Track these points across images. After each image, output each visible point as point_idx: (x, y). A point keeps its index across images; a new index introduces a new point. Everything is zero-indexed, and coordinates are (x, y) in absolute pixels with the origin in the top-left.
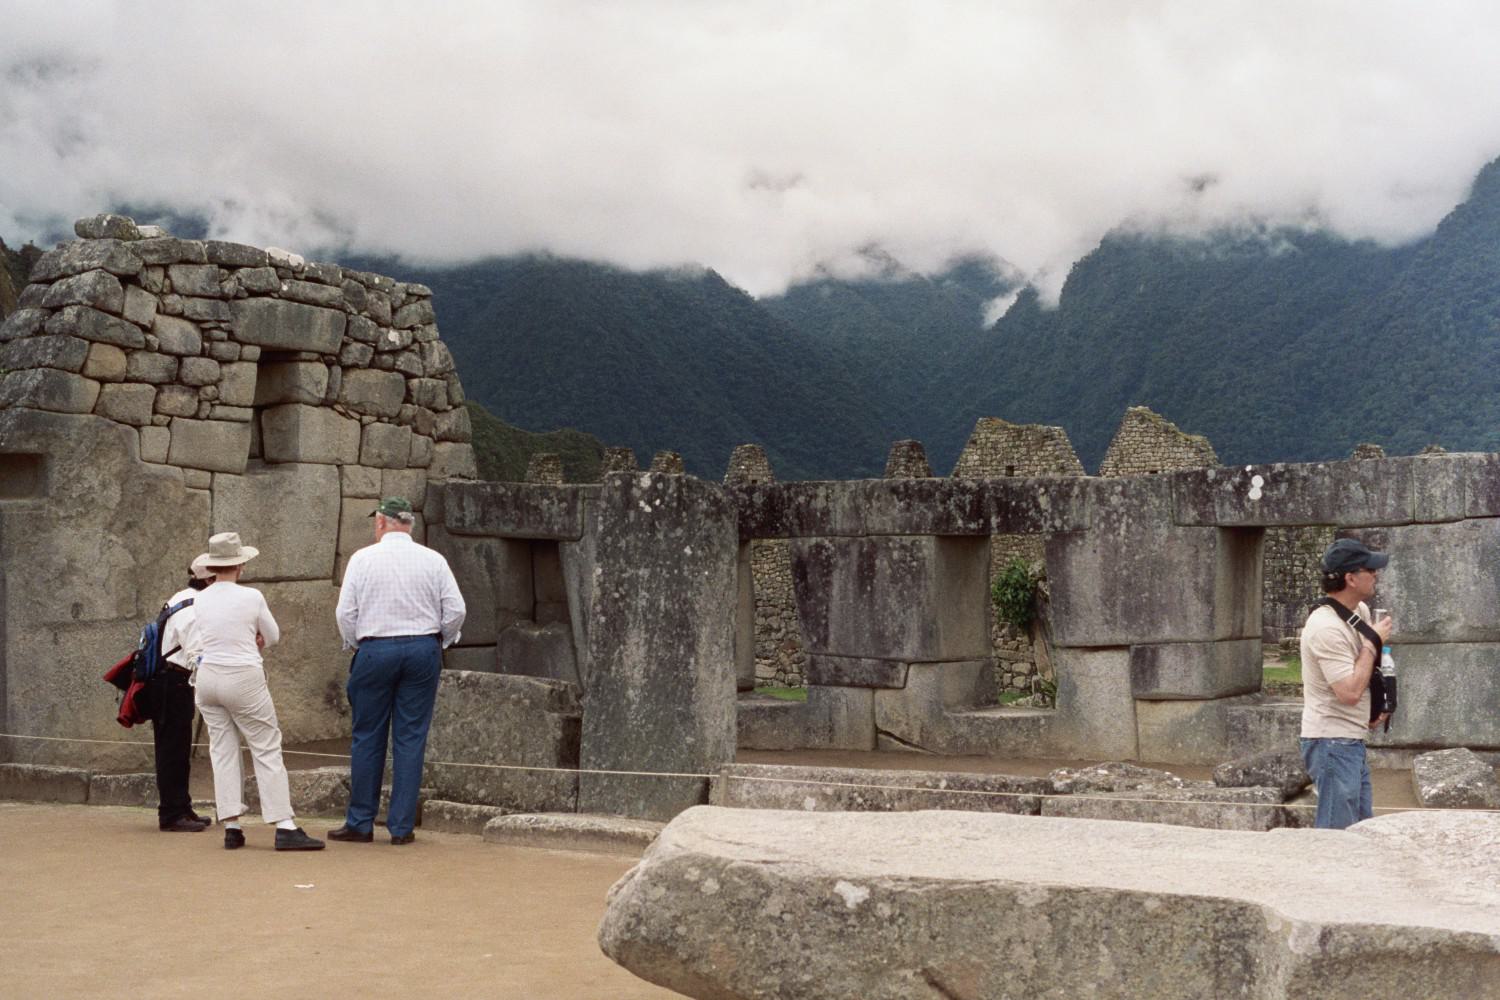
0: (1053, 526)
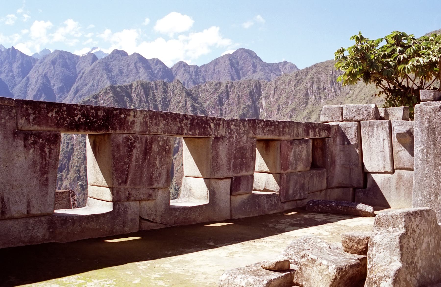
0: (214, 135)
